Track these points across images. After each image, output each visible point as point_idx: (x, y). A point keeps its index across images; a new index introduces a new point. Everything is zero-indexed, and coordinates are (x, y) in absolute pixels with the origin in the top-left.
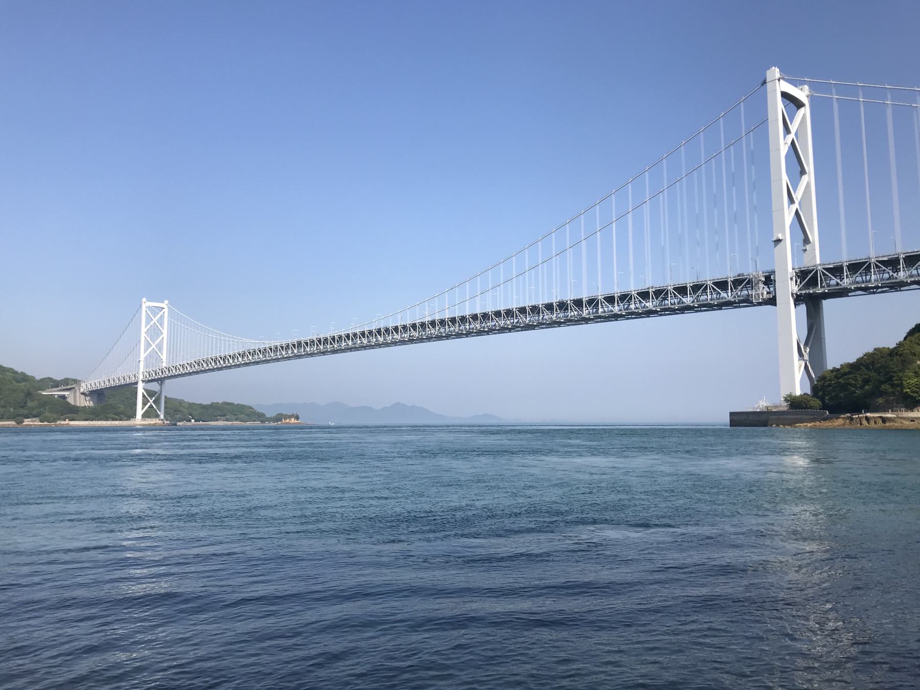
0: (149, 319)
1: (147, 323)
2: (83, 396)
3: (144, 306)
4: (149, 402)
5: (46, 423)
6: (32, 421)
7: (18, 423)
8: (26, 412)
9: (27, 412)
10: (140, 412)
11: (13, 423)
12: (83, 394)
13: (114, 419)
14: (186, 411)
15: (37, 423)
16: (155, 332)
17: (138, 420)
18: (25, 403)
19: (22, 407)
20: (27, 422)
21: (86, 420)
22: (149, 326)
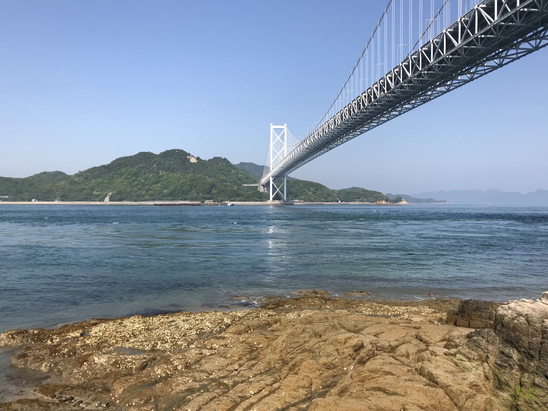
0: (274, 138)
1: (274, 140)
2: (262, 187)
3: (272, 131)
4: (277, 190)
5: (216, 203)
6: (209, 202)
7: (202, 203)
8: (209, 196)
9: (210, 196)
10: (271, 197)
11: (200, 202)
12: (262, 185)
13: (256, 201)
14: (335, 195)
15: (211, 202)
16: (279, 146)
17: (270, 201)
18: (210, 191)
19: (208, 193)
20: (207, 202)
21: (240, 201)
22: (274, 143)
